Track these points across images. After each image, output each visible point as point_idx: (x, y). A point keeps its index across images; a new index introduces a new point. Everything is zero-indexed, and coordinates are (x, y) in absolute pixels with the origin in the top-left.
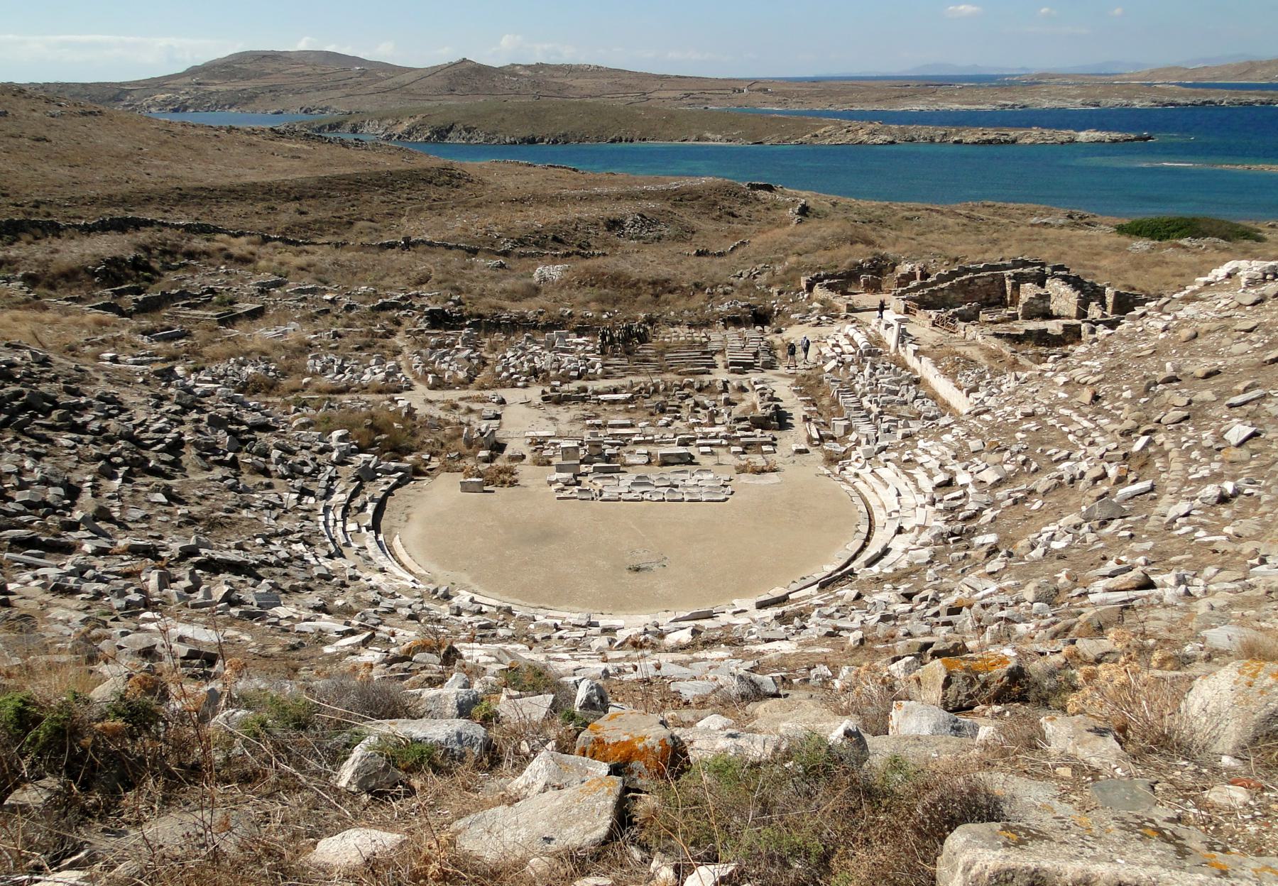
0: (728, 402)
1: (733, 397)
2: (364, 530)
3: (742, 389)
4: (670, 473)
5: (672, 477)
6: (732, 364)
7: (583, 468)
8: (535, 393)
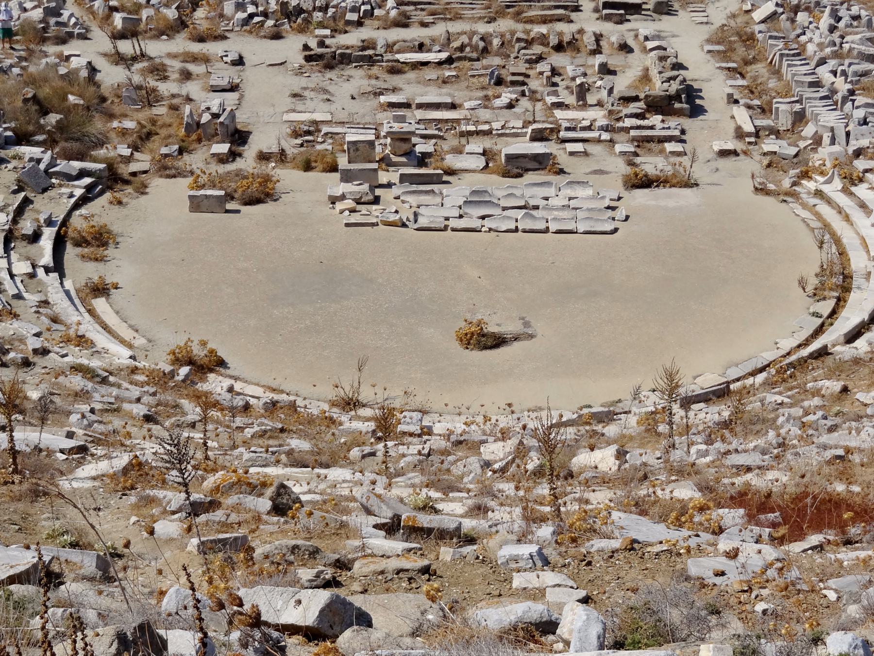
0: (606, 70)
1: (615, 60)
2: (41, 272)
3: (625, 48)
4: (529, 188)
5: (529, 192)
6: (606, 5)
7: (383, 177)
8: (291, 48)
